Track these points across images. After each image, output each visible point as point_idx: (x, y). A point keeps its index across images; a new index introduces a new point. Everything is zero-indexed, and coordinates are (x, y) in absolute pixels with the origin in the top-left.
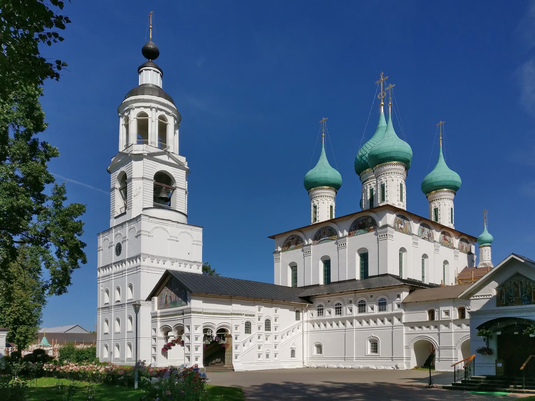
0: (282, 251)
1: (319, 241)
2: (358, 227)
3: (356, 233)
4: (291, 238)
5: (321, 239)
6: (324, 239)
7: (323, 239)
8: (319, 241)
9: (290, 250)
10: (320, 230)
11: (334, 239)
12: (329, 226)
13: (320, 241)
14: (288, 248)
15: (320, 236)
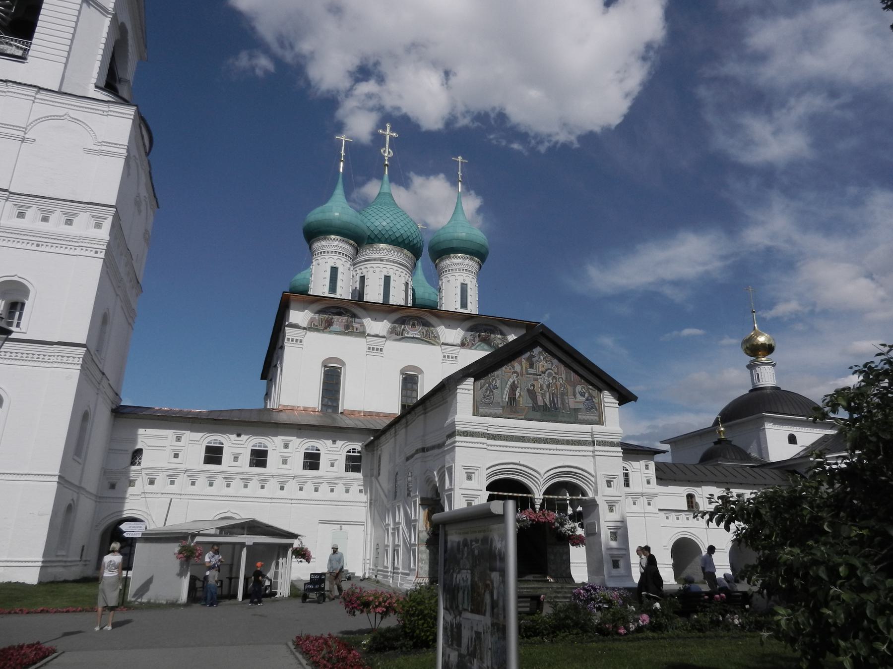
0: (312, 327)
1: (401, 337)
2: (478, 337)
3: (475, 346)
4: (335, 312)
5: (406, 335)
6: (412, 336)
7: (408, 336)
8: (401, 337)
9: (330, 332)
10: (404, 318)
11: (433, 342)
12: (424, 319)
13: (403, 338)
14: (326, 328)
15: (403, 330)
